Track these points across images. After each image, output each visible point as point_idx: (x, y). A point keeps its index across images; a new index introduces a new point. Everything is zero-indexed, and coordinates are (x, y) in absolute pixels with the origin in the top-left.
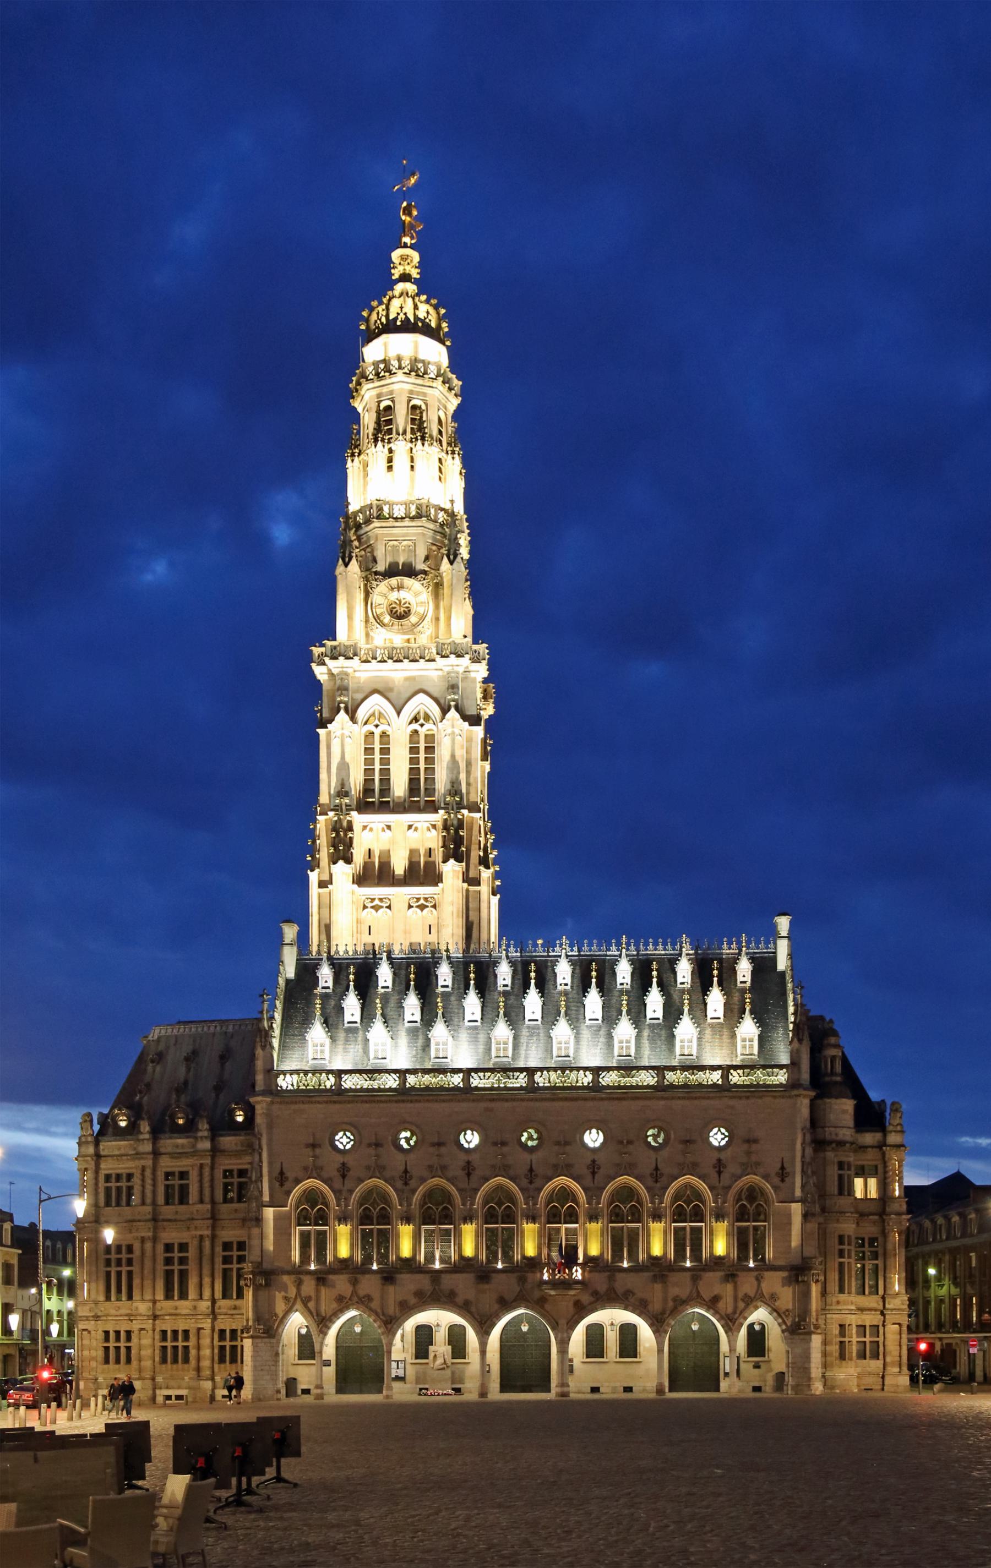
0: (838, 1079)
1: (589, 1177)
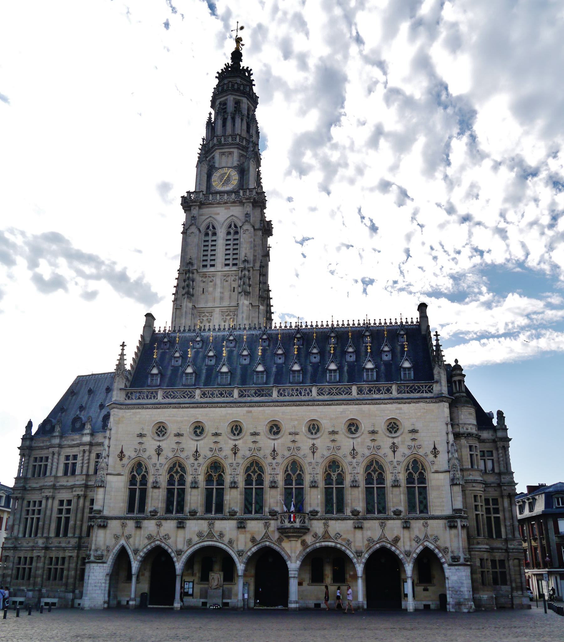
0: (464, 394)
1: (311, 454)
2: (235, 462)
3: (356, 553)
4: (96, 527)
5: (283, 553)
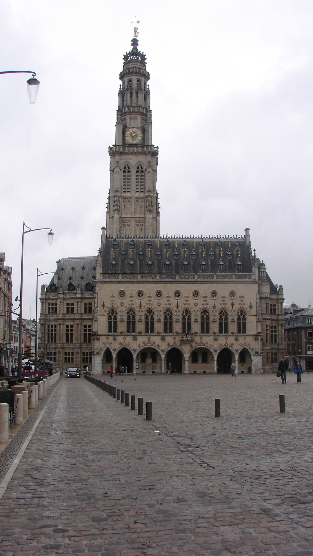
2: (159, 310)
3: (215, 350)
4: (95, 339)
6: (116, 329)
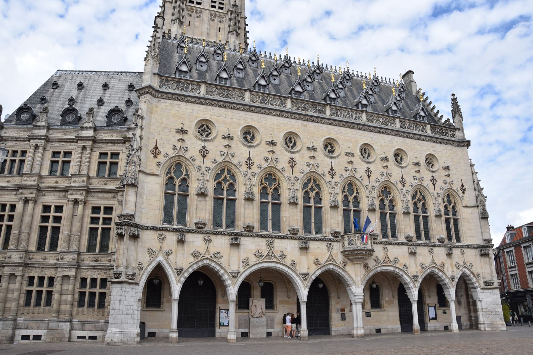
4: (127, 237)
5: (347, 277)
6: (185, 213)
